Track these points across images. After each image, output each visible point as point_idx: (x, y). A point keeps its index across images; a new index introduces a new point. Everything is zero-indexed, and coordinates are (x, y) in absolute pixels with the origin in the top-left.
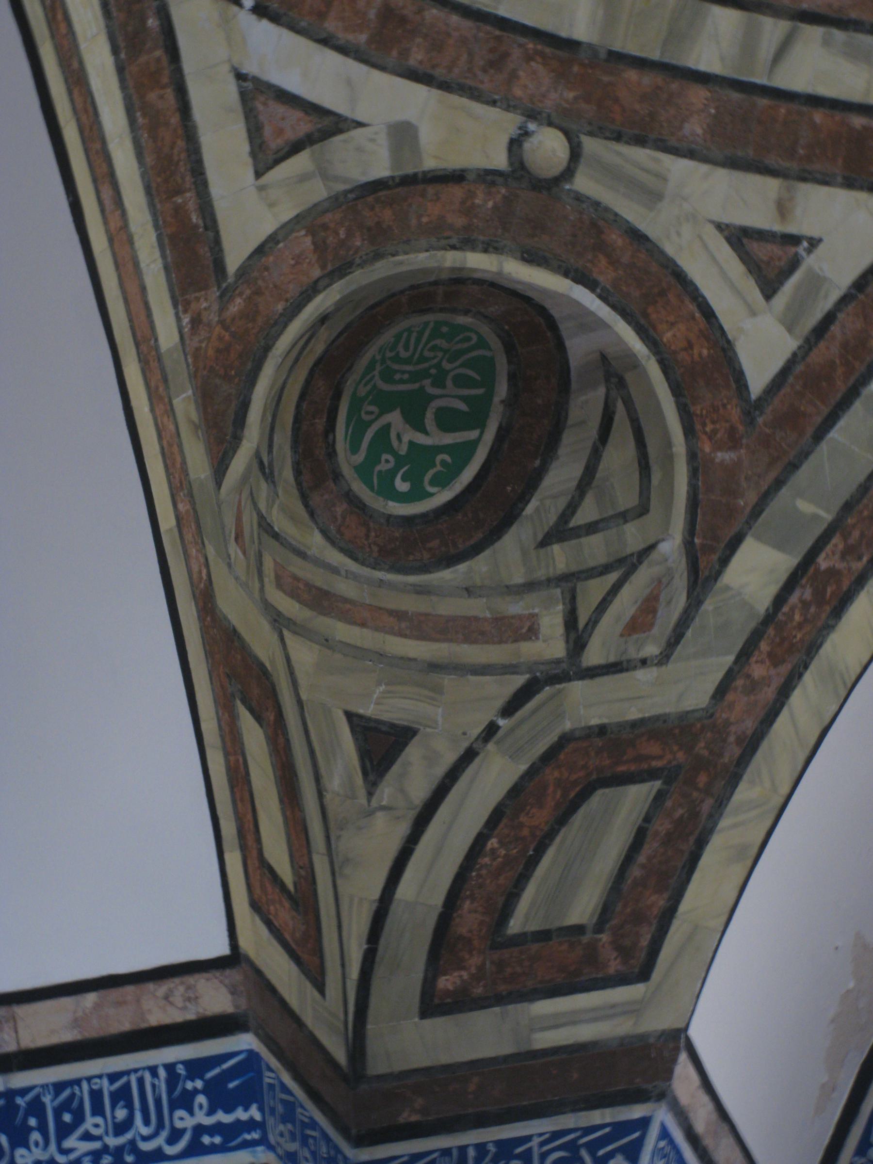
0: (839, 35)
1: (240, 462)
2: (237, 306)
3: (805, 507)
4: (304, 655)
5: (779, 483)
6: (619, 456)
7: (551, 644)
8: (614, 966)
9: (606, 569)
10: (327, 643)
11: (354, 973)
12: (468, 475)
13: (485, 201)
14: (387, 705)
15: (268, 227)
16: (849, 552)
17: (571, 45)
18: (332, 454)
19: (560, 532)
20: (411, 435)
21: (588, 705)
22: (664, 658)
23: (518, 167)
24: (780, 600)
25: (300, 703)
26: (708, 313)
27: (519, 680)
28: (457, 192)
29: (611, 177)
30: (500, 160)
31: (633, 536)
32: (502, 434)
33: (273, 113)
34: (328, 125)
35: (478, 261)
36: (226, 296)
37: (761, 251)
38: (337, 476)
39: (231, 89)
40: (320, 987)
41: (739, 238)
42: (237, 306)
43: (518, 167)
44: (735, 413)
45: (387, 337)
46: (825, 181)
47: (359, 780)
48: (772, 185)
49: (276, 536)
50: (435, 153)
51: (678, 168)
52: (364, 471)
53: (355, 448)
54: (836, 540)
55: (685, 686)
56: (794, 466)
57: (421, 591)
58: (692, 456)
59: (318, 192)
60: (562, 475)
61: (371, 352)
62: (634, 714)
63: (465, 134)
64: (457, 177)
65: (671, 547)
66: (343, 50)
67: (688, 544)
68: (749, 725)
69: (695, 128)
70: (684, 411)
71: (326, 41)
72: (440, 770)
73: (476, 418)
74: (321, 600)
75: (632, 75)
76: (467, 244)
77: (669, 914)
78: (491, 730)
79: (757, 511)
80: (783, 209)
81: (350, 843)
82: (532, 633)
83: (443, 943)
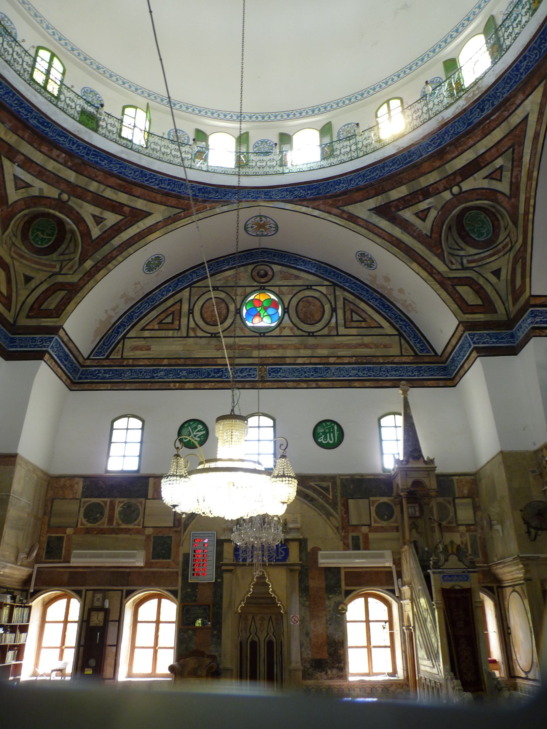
0: (113, 190)
1: (7, 233)
2: (10, 209)
3: (98, 257)
4: (16, 264)
5: (95, 253)
6: (72, 245)
7: (57, 270)
8: (55, 315)
9: (67, 260)
10: (21, 263)
11: (18, 310)
12: (50, 243)
13: (54, 203)
14: (29, 273)
15: (16, 198)
16: (102, 264)
17: (70, 182)
18: (28, 236)
19: (62, 254)
20: (42, 236)
21: (60, 279)
22: (72, 274)
23: (60, 199)
24: (91, 269)
25: (15, 271)
26: (88, 226)
27: (51, 274)
28: (49, 200)
29: (74, 203)
30: (57, 197)
31: (72, 256)
32: (56, 239)
33: (19, 182)
34: (28, 186)
35: (51, 211)
36: (8, 208)
37: (97, 219)
38: (29, 239)
39: (12, 177)
40: (9, 310)
41: (94, 216)
42: (10, 209)
43: (60, 199)
44: (90, 241)
45: (38, 220)
46: (108, 211)
47: (23, 283)
48: (100, 210)
49: (16, 246)
50: (46, 193)
51: (85, 204)
52: (34, 239)
53: (32, 236)
54: (101, 262)
55: (75, 279)
56: (97, 251)
57: (40, 258)
58: (82, 246)
59: (26, 195)
60: (64, 246)
61: (35, 222)
62: (66, 281)
63: (52, 192)
64: (49, 198)
65: (77, 259)
66: (32, 175)
67: (79, 258)
68: (82, 285)
69: (89, 198)
70: (82, 239)
71: (29, 173)
72: (37, 284)
73: (52, 235)
74: (22, 256)
75: (79, 189)
76: (50, 208)
77: (64, 309)
78: (45, 280)
79: (91, 256)
80: (101, 213)
81: (20, 292)
82: (55, 267)
83: (31, 308)
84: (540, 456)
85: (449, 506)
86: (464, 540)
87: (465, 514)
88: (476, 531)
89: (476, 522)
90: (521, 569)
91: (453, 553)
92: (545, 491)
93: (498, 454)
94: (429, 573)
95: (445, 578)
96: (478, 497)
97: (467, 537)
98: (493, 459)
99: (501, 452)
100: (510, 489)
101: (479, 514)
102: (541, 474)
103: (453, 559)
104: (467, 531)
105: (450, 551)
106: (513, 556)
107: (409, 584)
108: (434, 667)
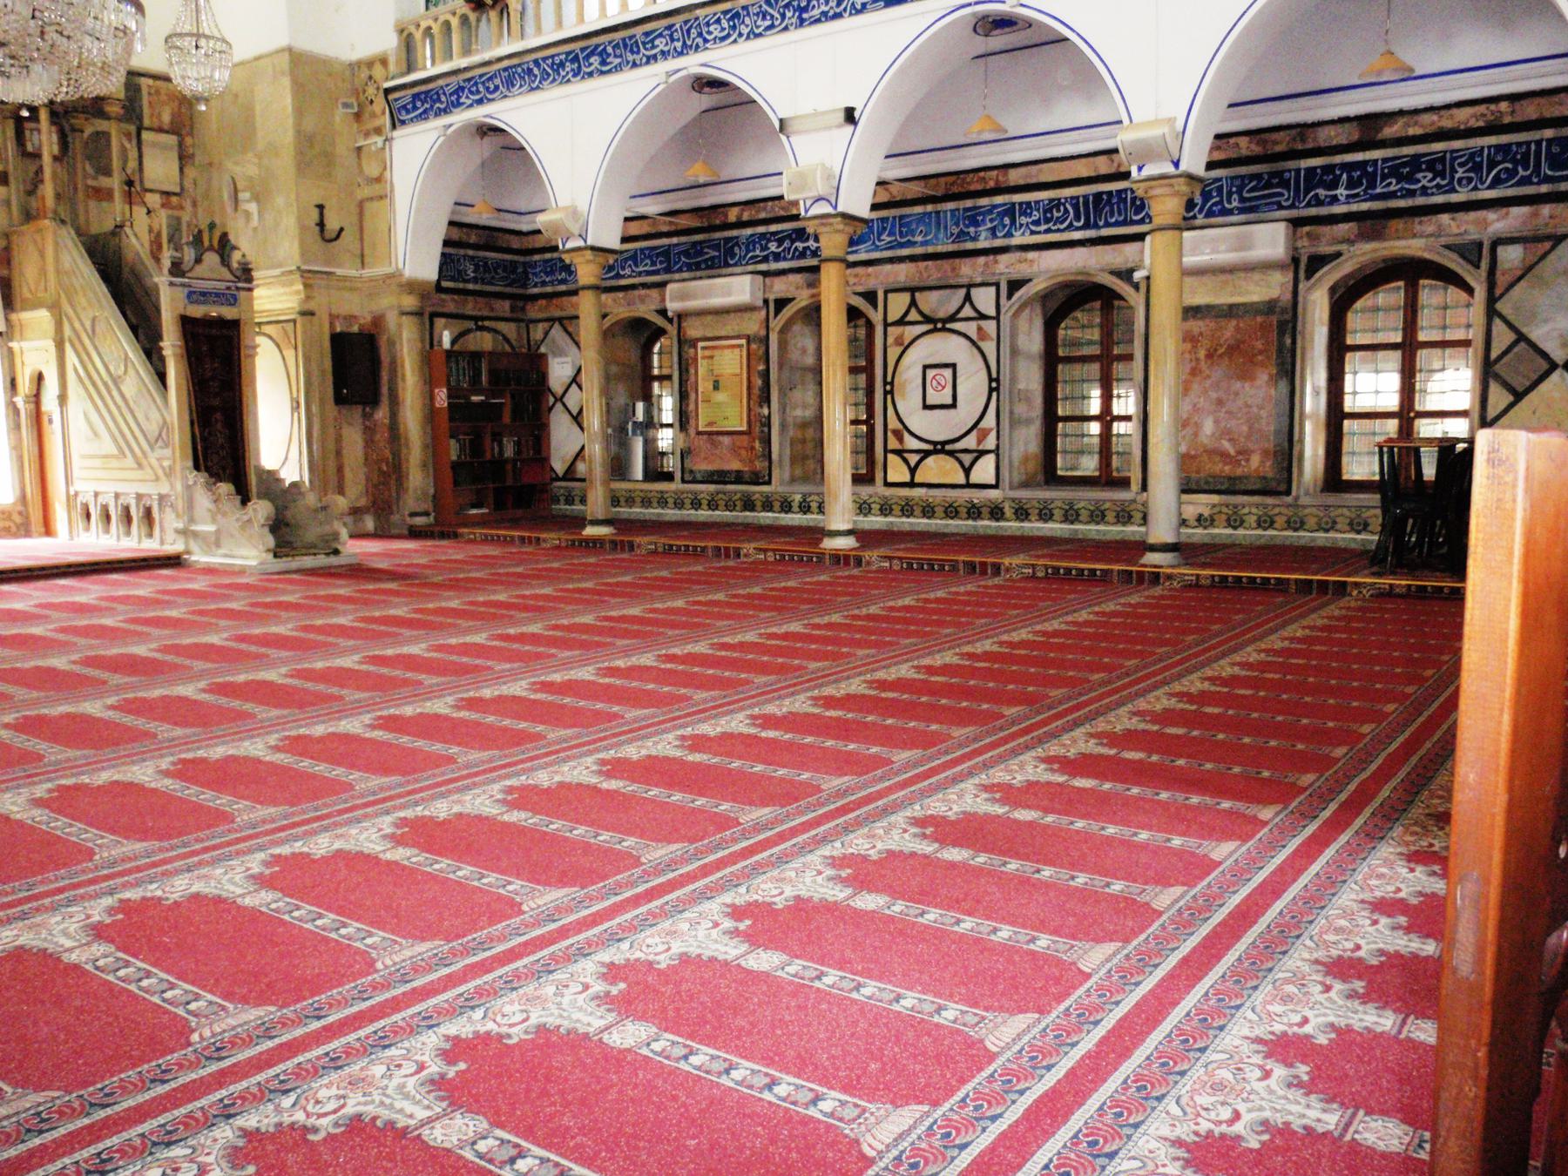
84: (364, 74)
85: (128, 146)
86: (156, 227)
87: (160, 168)
88: (182, 208)
89: (182, 189)
90: (298, 292)
91: (211, 248)
92: (359, 149)
93: (278, 52)
94: (156, 285)
95: (195, 296)
96: (191, 134)
97: (162, 219)
98: (257, 59)
99: (290, 50)
100: (299, 132)
101: (191, 172)
102: (358, 116)
103: (211, 259)
104: (163, 206)
105: (206, 243)
106: (280, 266)
107: (55, 308)
108: (140, 466)
